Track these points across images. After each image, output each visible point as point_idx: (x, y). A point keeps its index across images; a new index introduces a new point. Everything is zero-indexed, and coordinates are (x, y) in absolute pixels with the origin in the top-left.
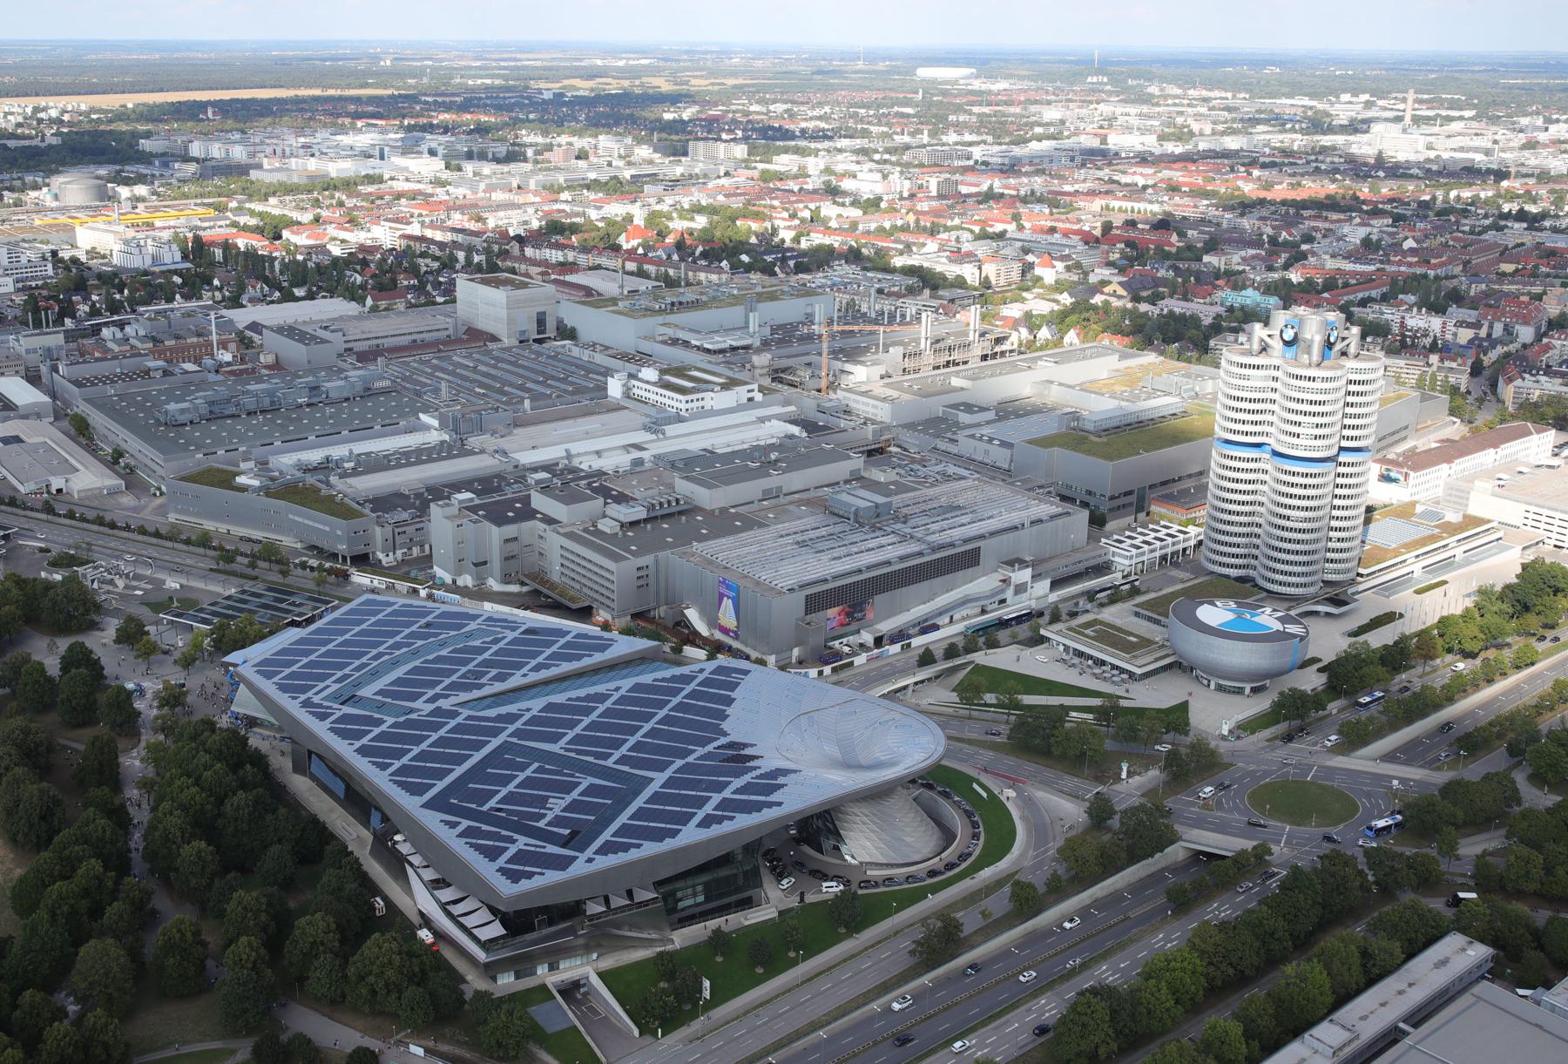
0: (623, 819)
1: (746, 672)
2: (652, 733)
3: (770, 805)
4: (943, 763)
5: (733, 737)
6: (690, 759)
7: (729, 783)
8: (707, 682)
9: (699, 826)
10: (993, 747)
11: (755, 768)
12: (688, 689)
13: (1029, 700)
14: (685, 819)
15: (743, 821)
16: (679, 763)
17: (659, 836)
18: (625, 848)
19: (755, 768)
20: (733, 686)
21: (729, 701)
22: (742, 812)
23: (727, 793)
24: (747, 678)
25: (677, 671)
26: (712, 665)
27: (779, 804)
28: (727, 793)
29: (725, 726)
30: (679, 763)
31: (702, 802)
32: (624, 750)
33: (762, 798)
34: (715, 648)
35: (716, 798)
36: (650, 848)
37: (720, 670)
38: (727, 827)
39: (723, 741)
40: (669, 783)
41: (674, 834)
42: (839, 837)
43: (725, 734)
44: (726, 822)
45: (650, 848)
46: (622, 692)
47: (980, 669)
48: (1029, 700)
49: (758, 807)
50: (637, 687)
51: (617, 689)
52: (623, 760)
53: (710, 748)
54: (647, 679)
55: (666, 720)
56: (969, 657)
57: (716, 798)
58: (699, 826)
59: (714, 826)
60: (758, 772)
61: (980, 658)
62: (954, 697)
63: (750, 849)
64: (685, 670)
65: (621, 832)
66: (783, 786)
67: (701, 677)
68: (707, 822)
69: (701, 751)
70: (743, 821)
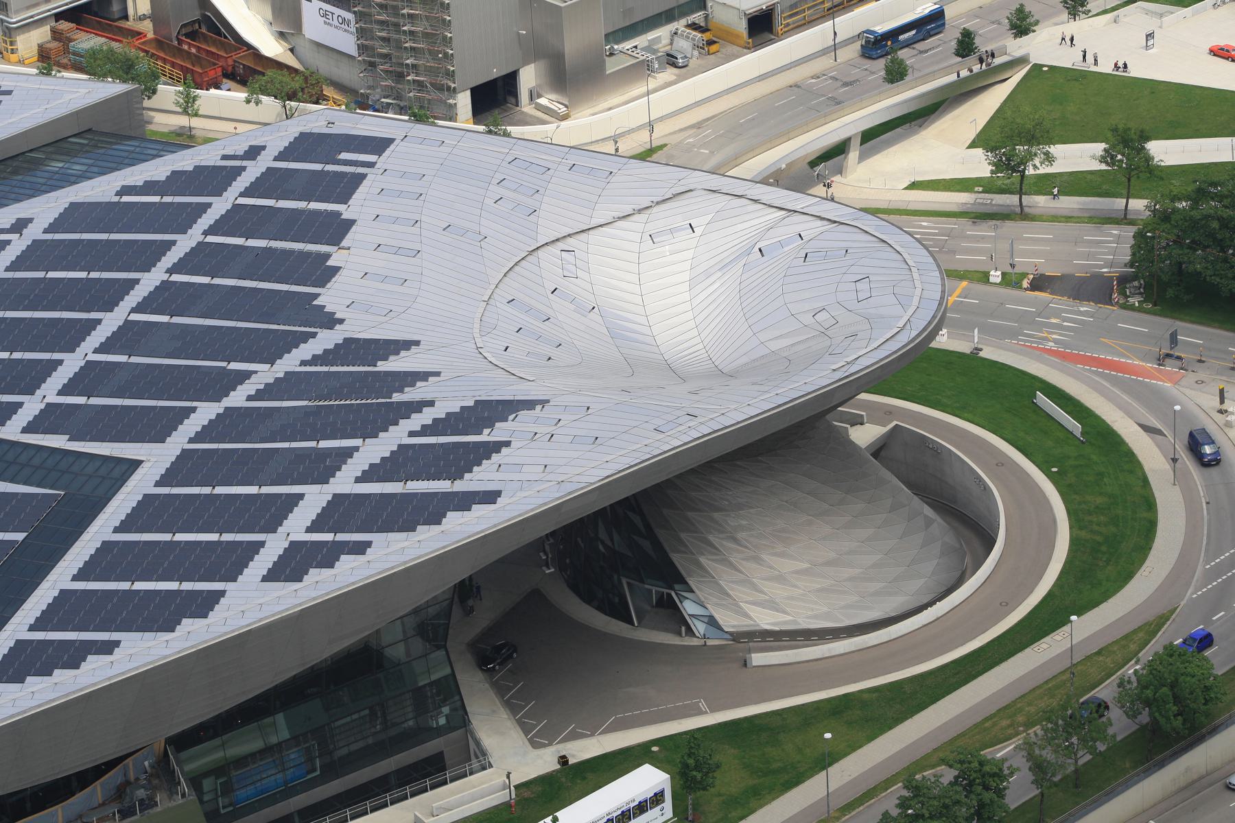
0: (61, 577)
1: (379, 145)
2: (125, 338)
3: (465, 501)
4: (943, 340)
5: (358, 326)
6: (237, 398)
7: (349, 453)
8: (268, 184)
9: (272, 576)
10: (1094, 289)
11: (418, 406)
12: (220, 206)
13: (1168, 152)
14: (231, 563)
15: (392, 552)
16: (206, 412)
17: (161, 615)
18: (73, 656)
19: (418, 406)
20: (345, 187)
21: (336, 230)
22: (387, 527)
23: (344, 482)
24: (383, 161)
25: (184, 161)
26: (278, 140)
27: (490, 497)
28: (344, 482)
29: (330, 298)
30: (206, 412)
31: (273, 513)
32: (50, 391)
33: (443, 486)
34: (297, 85)
35: (315, 498)
36: (140, 651)
37: (305, 145)
38: (350, 573)
39: (325, 340)
40: (184, 468)
41: (203, 605)
42: (675, 579)
43: (331, 321)
44: (347, 562)
45: (140, 651)
46: (35, 232)
47: (1042, 78)
48: (1168, 152)
49: (430, 511)
50: (74, 216)
51: (20, 226)
52: (48, 420)
53: (290, 362)
54: (100, 189)
55: (161, 299)
56: (1016, 47)
57: (315, 498)
58: (272, 576)
59: (314, 575)
60: (426, 417)
61: (1048, 46)
62: (980, 165)
63: (431, 626)
64: (207, 156)
65: (64, 610)
66: (497, 447)
67: (253, 171)
68: (292, 566)
69: (264, 374)
70: (392, 552)
